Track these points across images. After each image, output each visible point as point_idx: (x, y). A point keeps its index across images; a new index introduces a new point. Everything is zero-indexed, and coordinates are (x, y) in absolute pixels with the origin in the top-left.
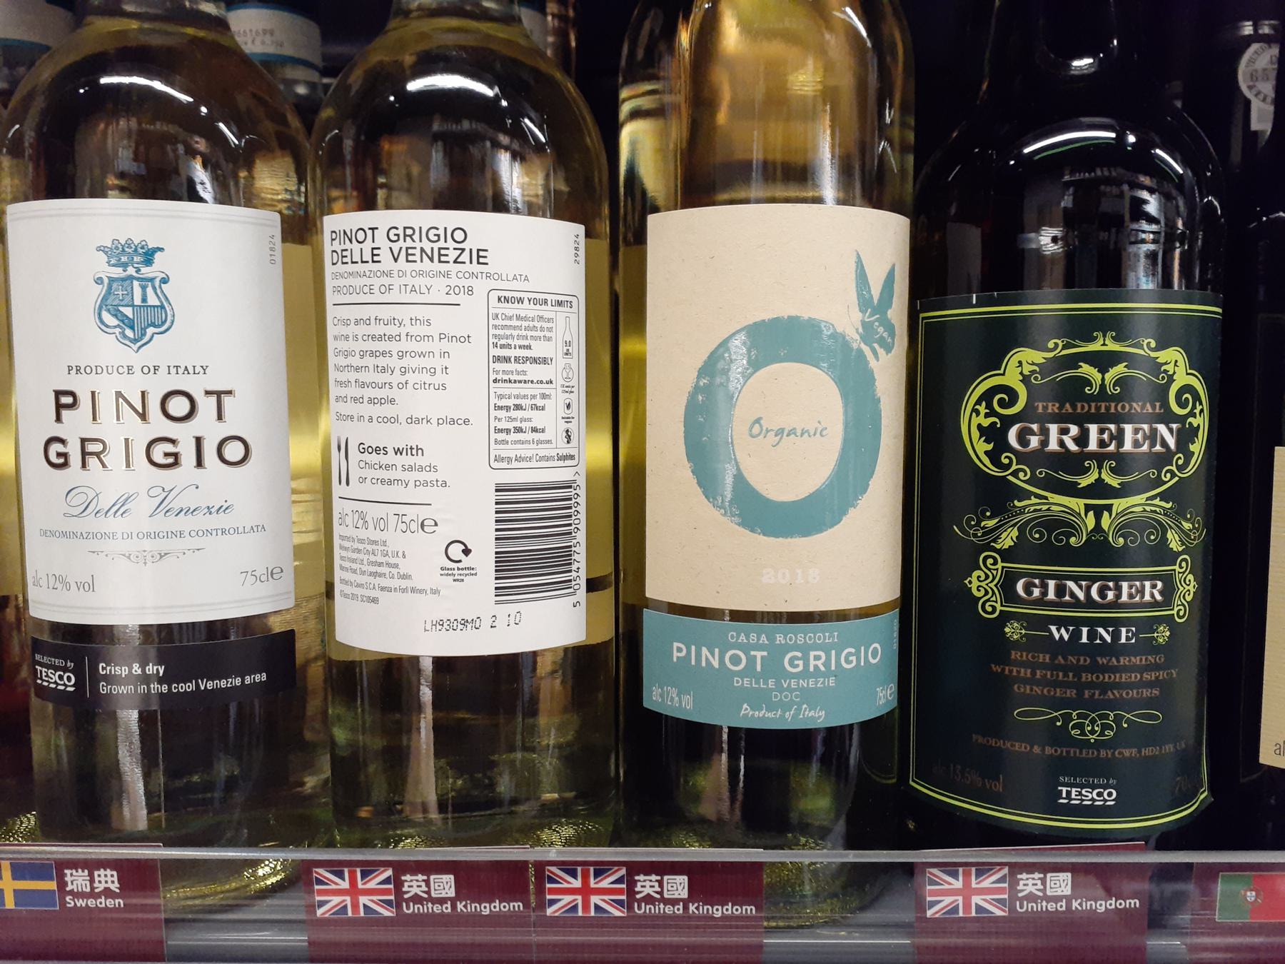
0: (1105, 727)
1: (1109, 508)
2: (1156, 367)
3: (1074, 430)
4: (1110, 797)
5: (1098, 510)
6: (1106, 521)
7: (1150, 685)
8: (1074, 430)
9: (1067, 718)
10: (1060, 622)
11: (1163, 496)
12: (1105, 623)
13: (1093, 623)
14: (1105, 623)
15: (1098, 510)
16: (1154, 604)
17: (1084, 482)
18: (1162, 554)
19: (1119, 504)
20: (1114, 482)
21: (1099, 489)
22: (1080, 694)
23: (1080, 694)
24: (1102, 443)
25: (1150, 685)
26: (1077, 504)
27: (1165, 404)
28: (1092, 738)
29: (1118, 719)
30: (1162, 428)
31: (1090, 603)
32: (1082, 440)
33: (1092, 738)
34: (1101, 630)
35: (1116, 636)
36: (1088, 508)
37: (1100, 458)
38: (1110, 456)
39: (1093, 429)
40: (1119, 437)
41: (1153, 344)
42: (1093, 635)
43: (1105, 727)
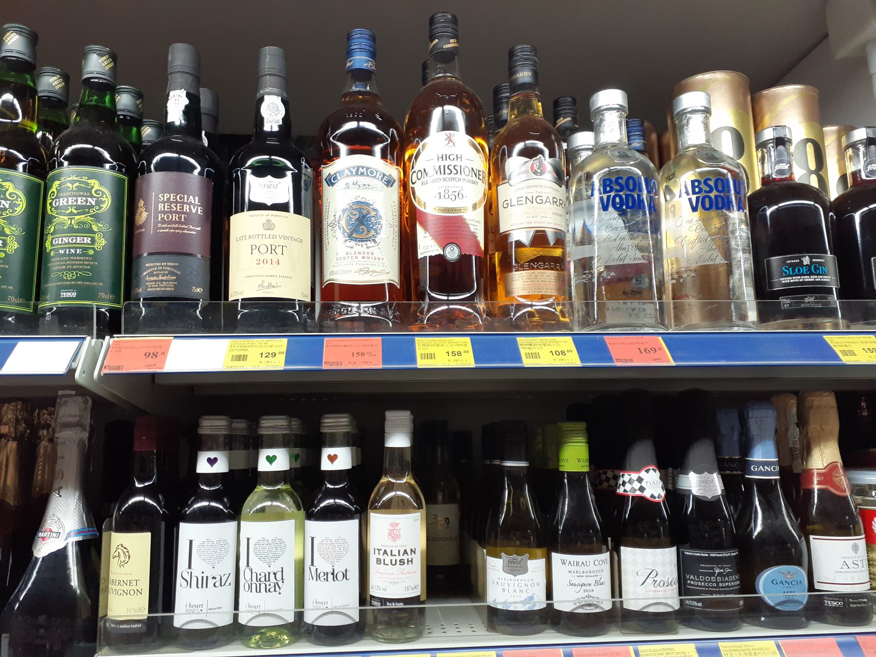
0: (73, 276)
1: (74, 218)
2: (88, 184)
3: (66, 199)
4: (74, 294)
5: (71, 219)
6: (73, 221)
7: (87, 265)
8: (66, 199)
9: (63, 274)
10: (62, 249)
11: (90, 216)
12: (73, 248)
13: (69, 248)
14: (73, 248)
15: (71, 219)
16: (88, 244)
17: (68, 212)
18: (91, 231)
19: (77, 217)
20: (75, 212)
21: (71, 214)
22: (66, 267)
23: (66, 267)
24: (72, 202)
25: (87, 265)
26: (66, 218)
27: (91, 193)
28: (69, 279)
29: (77, 274)
30: (89, 199)
31: (69, 243)
32: (67, 202)
33: (69, 279)
34: (72, 250)
35: (76, 251)
36: (69, 218)
37: (72, 206)
38: (74, 205)
39: (70, 199)
40: (77, 201)
41: (87, 178)
42: (69, 251)
43: (73, 276)
